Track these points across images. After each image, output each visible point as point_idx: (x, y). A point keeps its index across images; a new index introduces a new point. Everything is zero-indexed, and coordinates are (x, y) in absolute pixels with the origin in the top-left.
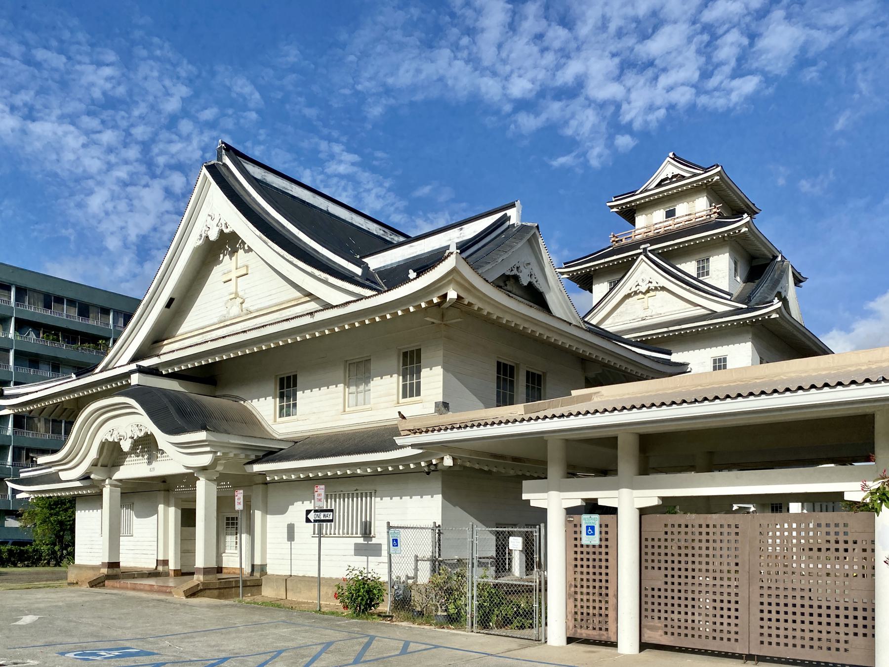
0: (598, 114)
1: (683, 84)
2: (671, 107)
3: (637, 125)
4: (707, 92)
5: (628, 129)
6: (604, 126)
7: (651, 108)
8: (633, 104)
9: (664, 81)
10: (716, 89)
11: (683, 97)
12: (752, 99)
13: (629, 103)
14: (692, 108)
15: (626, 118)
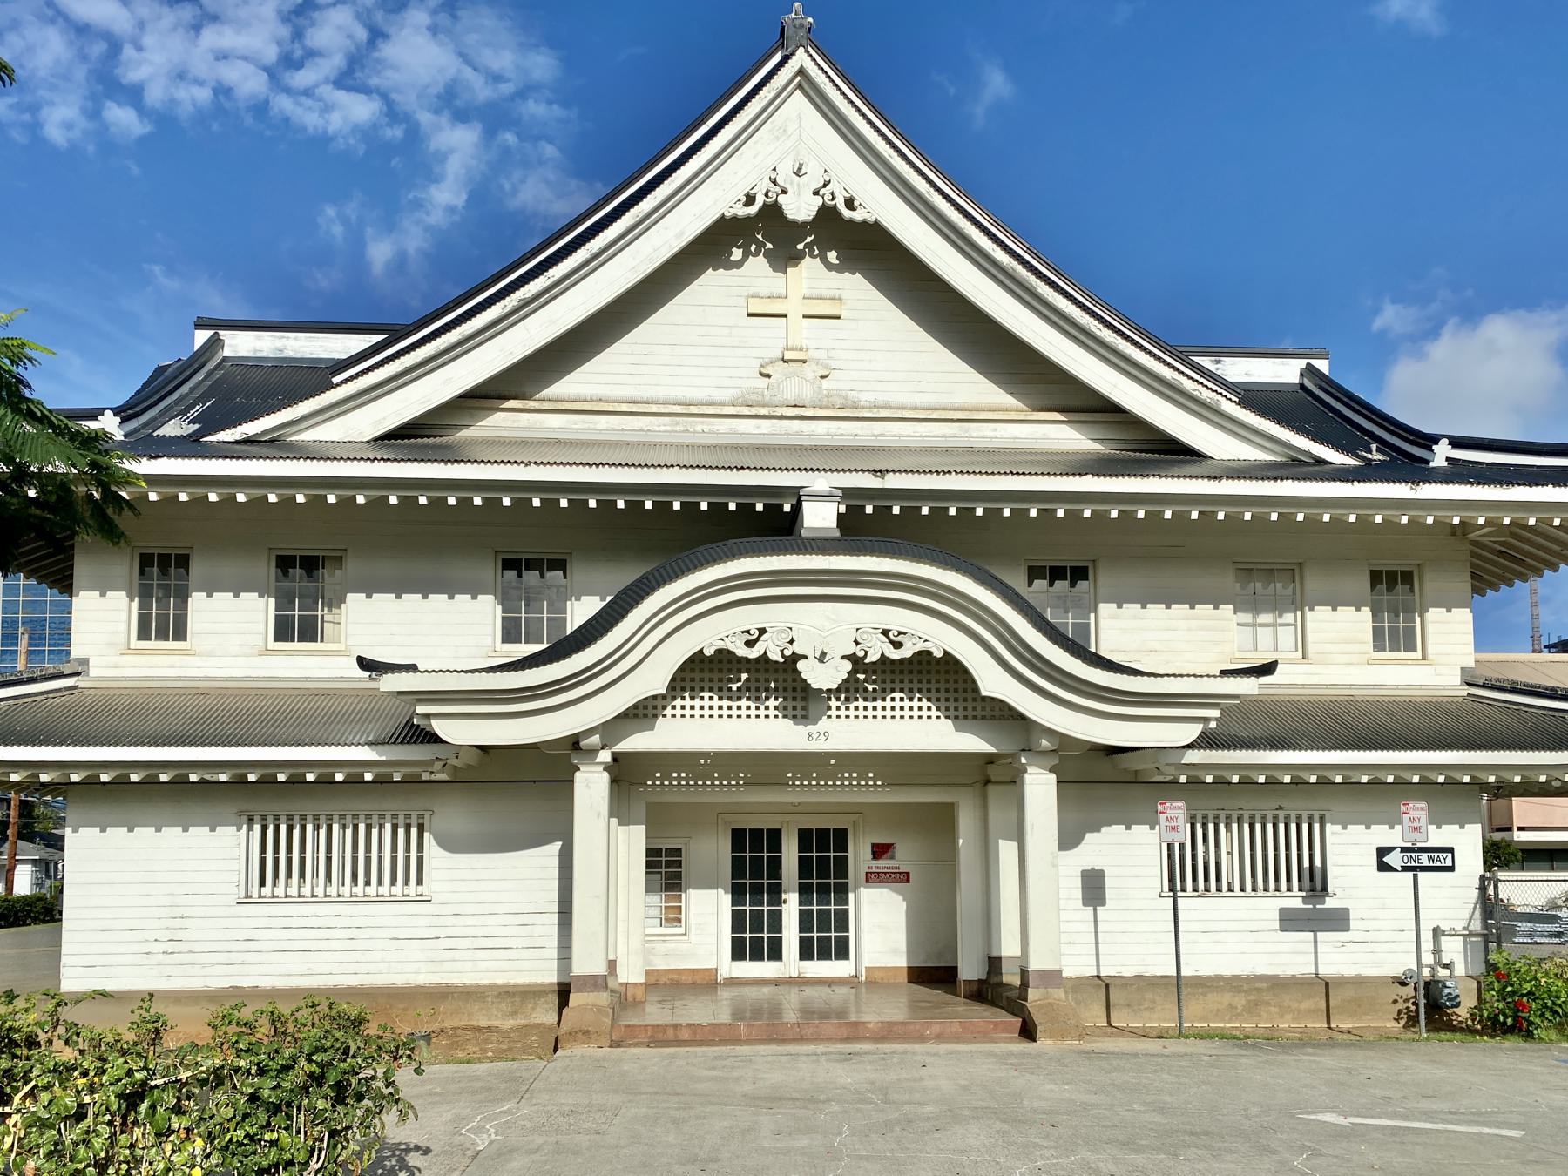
0: (71, 43)
1: (246, 59)
2: (223, 91)
3: (155, 95)
4: (288, 91)
5: (133, 95)
6: (80, 73)
7: (181, 76)
8: (144, 55)
9: (211, 37)
10: (308, 92)
11: (249, 82)
12: (368, 133)
13: (139, 48)
14: (261, 108)
15: (133, 76)
